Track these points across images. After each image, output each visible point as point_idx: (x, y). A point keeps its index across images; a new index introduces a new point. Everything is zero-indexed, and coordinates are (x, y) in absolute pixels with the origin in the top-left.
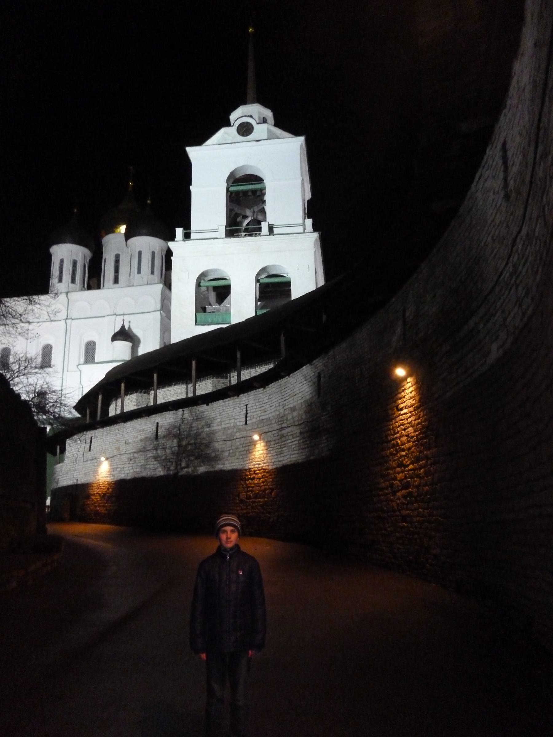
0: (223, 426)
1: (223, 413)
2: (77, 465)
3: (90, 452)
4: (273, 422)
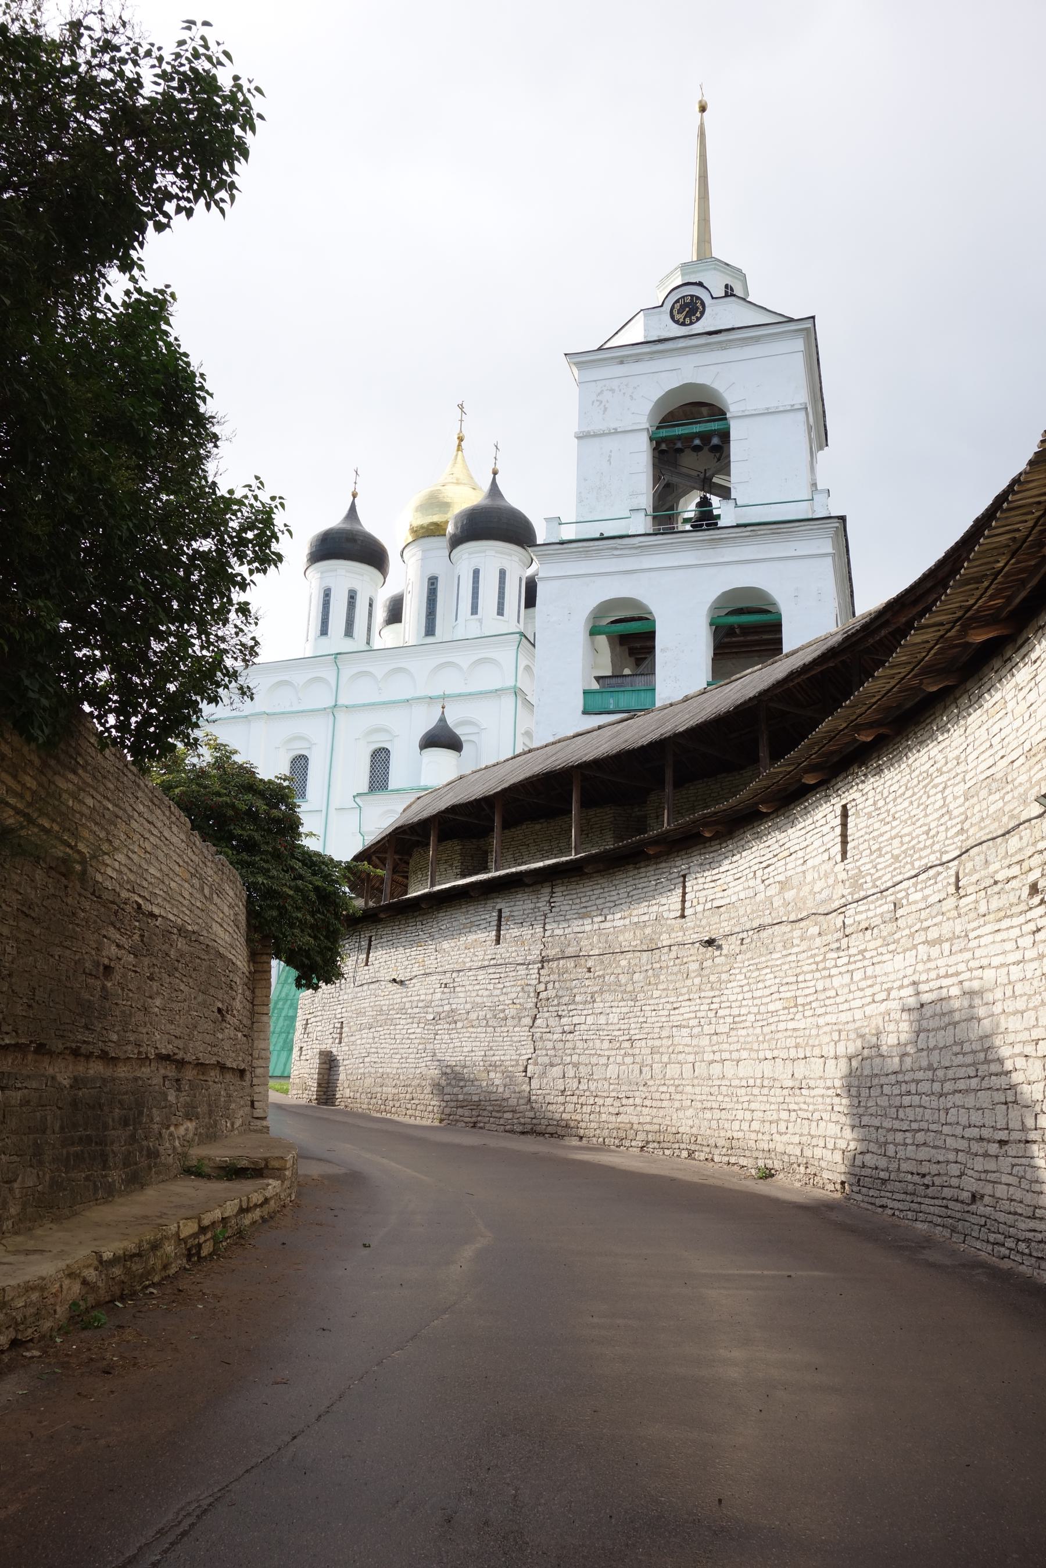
0: (636, 920)
1: (635, 892)
2: (342, 993)
3: (366, 968)
4: (741, 912)
